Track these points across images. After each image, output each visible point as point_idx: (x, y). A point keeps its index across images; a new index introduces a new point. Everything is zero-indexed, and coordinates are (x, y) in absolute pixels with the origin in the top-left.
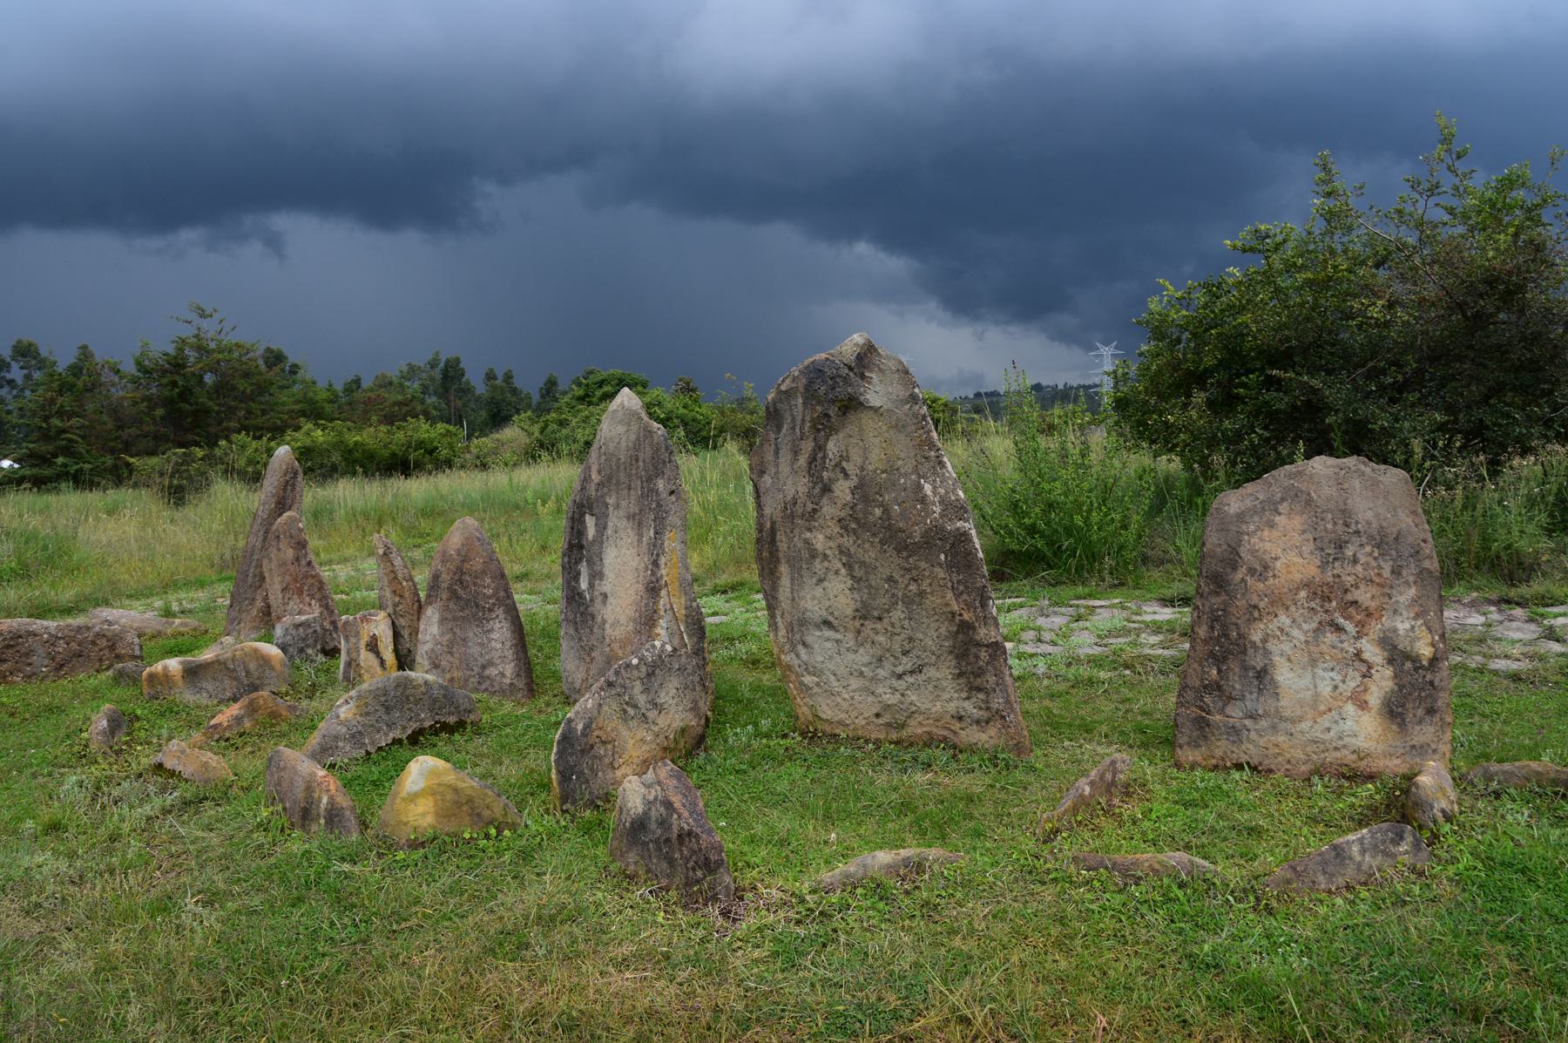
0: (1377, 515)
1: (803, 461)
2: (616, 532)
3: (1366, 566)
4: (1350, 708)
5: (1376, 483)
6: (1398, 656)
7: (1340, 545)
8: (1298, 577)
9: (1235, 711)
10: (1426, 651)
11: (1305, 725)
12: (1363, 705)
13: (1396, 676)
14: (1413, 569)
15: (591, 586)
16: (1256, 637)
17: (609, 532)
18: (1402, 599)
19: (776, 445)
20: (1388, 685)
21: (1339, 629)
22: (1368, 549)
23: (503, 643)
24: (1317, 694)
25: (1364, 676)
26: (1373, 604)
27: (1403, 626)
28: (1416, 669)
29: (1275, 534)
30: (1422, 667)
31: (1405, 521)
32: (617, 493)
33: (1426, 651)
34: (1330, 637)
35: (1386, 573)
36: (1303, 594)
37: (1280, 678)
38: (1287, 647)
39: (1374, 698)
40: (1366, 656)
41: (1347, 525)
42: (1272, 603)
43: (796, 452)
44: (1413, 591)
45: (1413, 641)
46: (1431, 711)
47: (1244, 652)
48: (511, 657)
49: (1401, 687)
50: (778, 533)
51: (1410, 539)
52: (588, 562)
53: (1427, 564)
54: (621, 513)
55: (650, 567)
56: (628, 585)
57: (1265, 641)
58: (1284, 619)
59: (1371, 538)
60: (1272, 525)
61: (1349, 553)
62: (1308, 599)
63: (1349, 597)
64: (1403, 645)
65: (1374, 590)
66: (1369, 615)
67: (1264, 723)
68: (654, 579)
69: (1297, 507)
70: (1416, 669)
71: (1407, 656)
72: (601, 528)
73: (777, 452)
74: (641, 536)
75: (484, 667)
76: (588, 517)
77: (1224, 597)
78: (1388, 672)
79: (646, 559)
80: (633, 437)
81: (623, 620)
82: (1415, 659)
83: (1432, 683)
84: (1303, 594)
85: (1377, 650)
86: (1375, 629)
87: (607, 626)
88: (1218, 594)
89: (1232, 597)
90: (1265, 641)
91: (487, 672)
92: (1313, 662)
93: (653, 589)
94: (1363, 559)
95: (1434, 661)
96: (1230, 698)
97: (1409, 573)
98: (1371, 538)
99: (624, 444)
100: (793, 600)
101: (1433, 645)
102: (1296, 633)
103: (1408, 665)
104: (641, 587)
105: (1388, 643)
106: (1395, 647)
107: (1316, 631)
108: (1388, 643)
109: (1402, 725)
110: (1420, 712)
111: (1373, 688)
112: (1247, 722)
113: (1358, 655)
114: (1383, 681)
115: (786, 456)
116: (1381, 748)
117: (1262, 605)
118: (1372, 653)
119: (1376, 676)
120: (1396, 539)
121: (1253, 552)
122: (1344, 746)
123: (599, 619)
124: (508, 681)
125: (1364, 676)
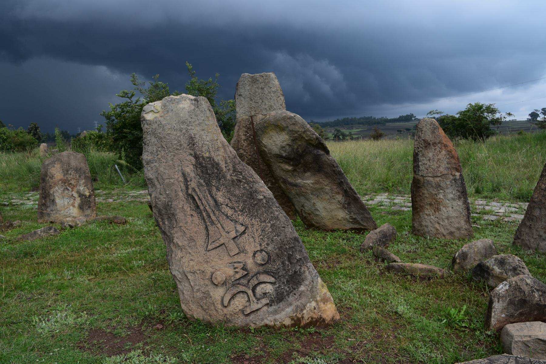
0: (76, 164)
3: (73, 175)
4: (71, 207)
5: (76, 157)
6: (81, 195)
7: (67, 171)
8: (59, 178)
9: (49, 210)
10: (87, 194)
11: (62, 212)
12: (74, 206)
13: (81, 200)
14: (84, 176)
16: (52, 192)
18: (81, 182)
20: (79, 202)
21: (68, 190)
22: (73, 172)
24: (64, 205)
26: (75, 184)
27: (82, 188)
28: (85, 198)
29: (55, 169)
30: (87, 197)
31: (82, 165)
33: (87, 194)
34: (66, 192)
35: (78, 177)
36: (60, 182)
37: (57, 201)
38: (58, 194)
39: (76, 205)
40: (74, 195)
41: (69, 166)
42: (54, 184)
44: (84, 181)
45: (84, 191)
46: (90, 207)
47: (49, 196)
49: (82, 202)
51: (83, 169)
53: (87, 175)
57: (53, 193)
58: (57, 188)
59: (74, 169)
60: (54, 167)
61: (69, 172)
62: (62, 183)
63: (70, 182)
64: (82, 193)
65: (75, 181)
66: (74, 186)
67: (54, 212)
69: (59, 163)
70: (85, 198)
71: (83, 195)
77: (45, 183)
78: (79, 199)
82: (85, 196)
83: (89, 201)
84: (60, 182)
85: (76, 194)
86: (75, 189)
88: (43, 183)
89: (46, 183)
90: (53, 193)
92: (63, 198)
94: (72, 174)
95: (90, 196)
96: (48, 207)
97: (83, 177)
98: (74, 169)
101: (89, 192)
102: (59, 191)
103: (84, 197)
105: (78, 192)
106: (80, 193)
107: (64, 190)
108: (78, 192)
109: (83, 210)
110: (87, 207)
111: (76, 203)
112: (51, 212)
113: (72, 195)
114: (78, 201)
116: (78, 215)
117: (52, 185)
118: (76, 195)
119: (76, 200)
120: (80, 169)
121: (50, 173)
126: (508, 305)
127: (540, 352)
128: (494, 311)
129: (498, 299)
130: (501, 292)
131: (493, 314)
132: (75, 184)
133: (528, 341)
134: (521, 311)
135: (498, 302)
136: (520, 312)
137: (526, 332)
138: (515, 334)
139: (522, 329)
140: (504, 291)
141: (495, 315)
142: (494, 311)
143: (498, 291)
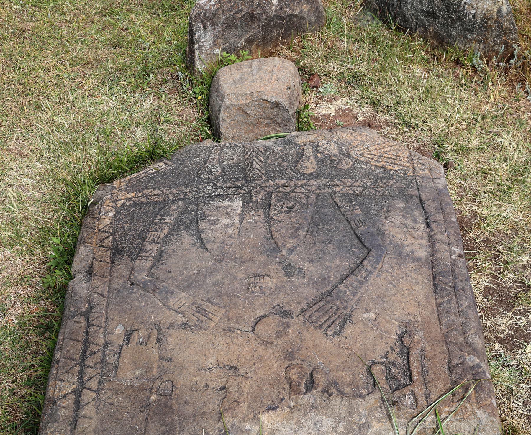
126: (224, 30)
127: (266, 121)
128: (200, 47)
129: (203, 23)
130: (207, 7)
131: (197, 53)
133: (247, 106)
134: (249, 35)
135: (205, 28)
136: (247, 39)
137: (247, 87)
138: (227, 92)
139: (241, 80)
140: (214, 5)
141: (201, 53)
142: (200, 47)
143: (202, 8)
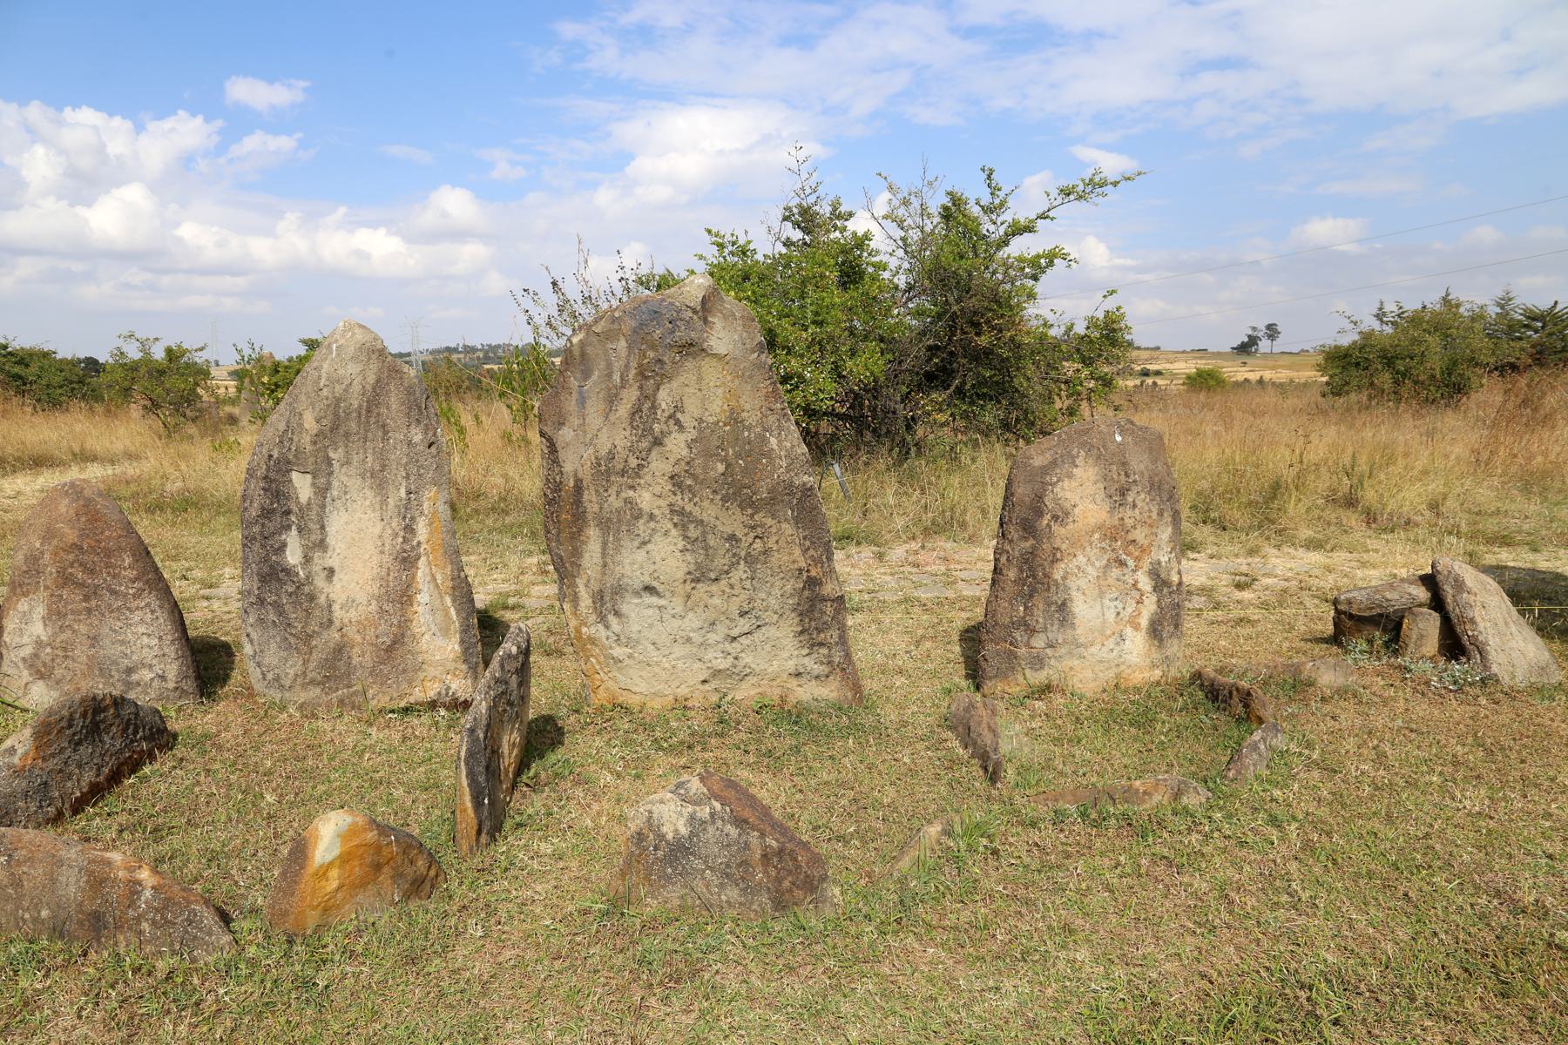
1: (623, 410)
2: (346, 493)
7: (1123, 492)
8: (1092, 521)
9: (1039, 642)
11: (1093, 650)
12: (1137, 627)
15: (307, 560)
16: (1057, 576)
17: (335, 493)
19: (580, 393)
20: (1153, 607)
21: (1122, 564)
22: (1143, 496)
23: (160, 638)
24: (1104, 622)
25: (1138, 603)
26: (1146, 542)
29: (1074, 484)
32: (346, 447)
34: (1115, 572)
35: (1154, 516)
36: (1097, 536)
37: (1076, 610)
38: (1082, 583)
39: (1144, 622)
40: (1140, 586)
41: (1127, 475)
42: (1073, 545)
43: (612, 399)
47: (1048, 590)
48: (173, 655)
50: (586, 492)
52: (300, 530)
54: (352, 470)
55: (402, 533)
56: (367, 556)
57: (1064, 578)
58: (1081, 559)
60: (1070, 476)
61: (1130, 499)
62: (1102, 540)
63: (1130, 537)
66: (1143, 551)
67: (1063, 651)
68: (407, 547)
69: (1090, 461)
72: (322, 491)
73: (582, 402)
74: (384, 502)
75: (129, 671)
76: (295, 476)
77: (1032, 542)
79: (394, 524)
80: (371, 379)
81: (362, 598)
84: (1097, 536)
87: (336, 607)
88: (1026, 539)
89: (1039, 541)
90: (1064, 578)
91: (135, 677)
92: (1101, 595)
93: (405, 560)
94: (1140, 504)
96: (1034, 631)
99: (357, 387)
100: (605, 565)
102: (1090, 569)
104: (387, 559)
107: (1107, 566)
109: (1161, 641)
112: (1048, 651)
115: (594, 409)
117: (1064, 547)
118: (1145, 583)
119: (1146, 602)
121: (1056, 501)
122: (1123, 663)
123: (322, 600)
124: (171, 685)
125: (1138, 603)
132: (1146, 542)
